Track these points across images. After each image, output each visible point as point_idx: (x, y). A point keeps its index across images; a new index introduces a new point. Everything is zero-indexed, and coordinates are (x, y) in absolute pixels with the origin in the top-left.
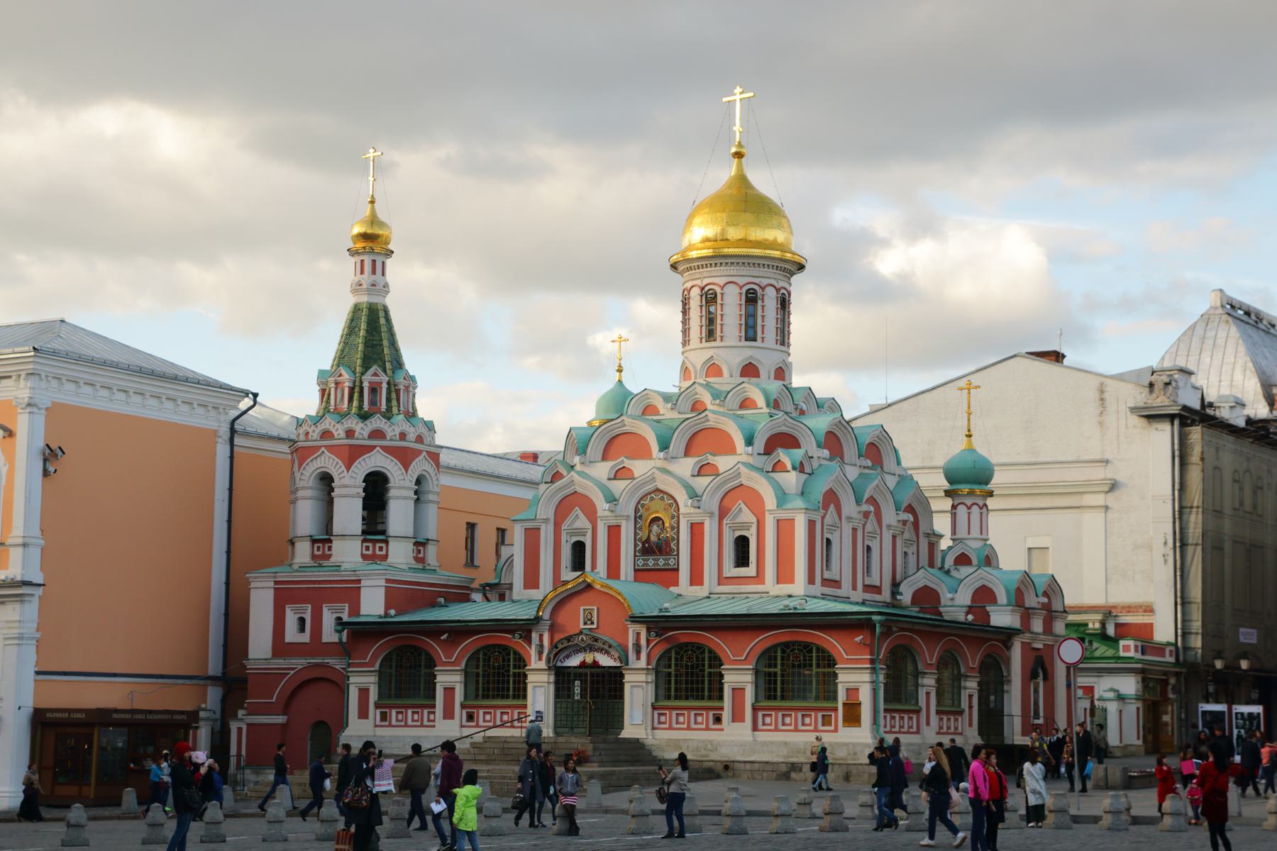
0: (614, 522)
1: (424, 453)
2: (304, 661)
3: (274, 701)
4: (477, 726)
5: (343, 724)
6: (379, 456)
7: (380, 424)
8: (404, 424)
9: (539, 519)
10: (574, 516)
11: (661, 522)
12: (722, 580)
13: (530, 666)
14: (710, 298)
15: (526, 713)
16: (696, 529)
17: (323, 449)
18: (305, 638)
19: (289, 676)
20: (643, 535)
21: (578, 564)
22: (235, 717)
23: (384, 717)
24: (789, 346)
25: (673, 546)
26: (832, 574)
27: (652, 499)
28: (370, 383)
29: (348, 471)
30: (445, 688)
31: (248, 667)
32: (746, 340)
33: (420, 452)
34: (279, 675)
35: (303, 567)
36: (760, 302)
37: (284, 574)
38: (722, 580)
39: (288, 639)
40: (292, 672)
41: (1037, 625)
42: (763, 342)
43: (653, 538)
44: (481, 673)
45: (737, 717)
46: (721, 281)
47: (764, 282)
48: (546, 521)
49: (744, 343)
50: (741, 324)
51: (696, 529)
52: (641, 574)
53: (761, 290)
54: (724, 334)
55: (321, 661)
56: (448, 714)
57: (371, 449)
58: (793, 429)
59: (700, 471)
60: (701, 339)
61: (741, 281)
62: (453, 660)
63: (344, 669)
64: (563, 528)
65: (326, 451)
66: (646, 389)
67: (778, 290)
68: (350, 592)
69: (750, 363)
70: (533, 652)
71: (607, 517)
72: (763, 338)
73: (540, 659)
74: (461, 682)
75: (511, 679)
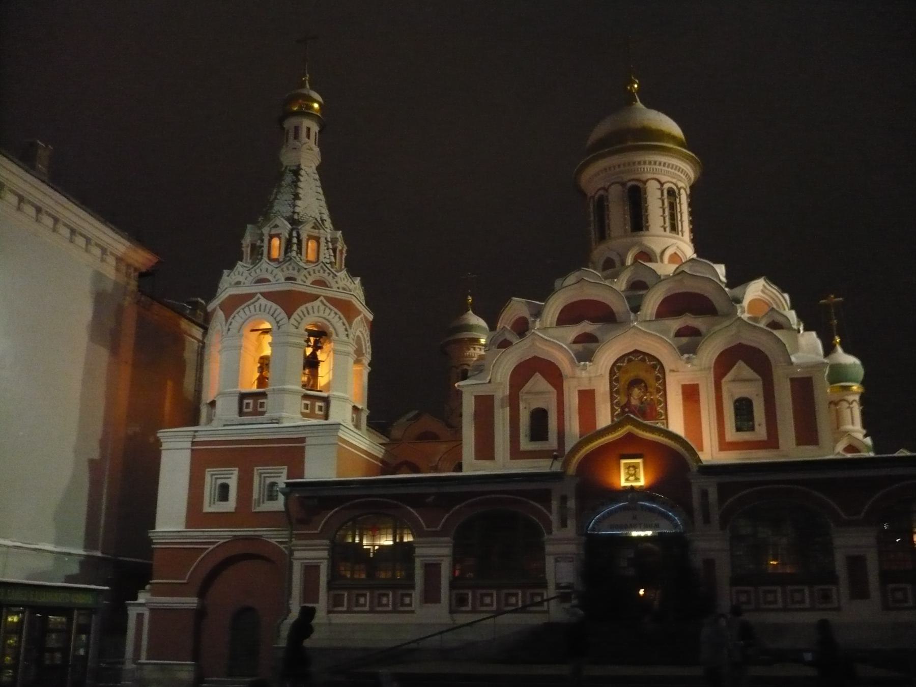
1: (362, 315)
2: (230, 533)
3: (185, 581)
4: (474, 611)
6: (322, 308)
7: (324, 273)
8: (345, 278)
11: (643, 385)
13: (550, 532)
15: (542, 595)
17: (259, 295)
18: (230, 505)
19: (205, 553)
20: (621, 399)
25: (659, 409)
27: (630, 361)
28: (308, 235)
29: (289, 318)
31: (154, 541)
32: (670, 232)
36: (678, 200)
37: (205, 431)
39: (207, 509)
40: (212, 547)
42: (682, 235)
43: (634, 402)
45: (859, 591)
47: (680, 184)
49: (668, 233)
51: (691, 394)
55: (252, 533)
56: (432, 595)
57: (315, 297)
61: (663, 179)
62: (439, 529)
63: (281, 543)
65: (262, 298)
69: (675, 253)
70: (554, 518)
73: (564, 524)
74: (450, 556)
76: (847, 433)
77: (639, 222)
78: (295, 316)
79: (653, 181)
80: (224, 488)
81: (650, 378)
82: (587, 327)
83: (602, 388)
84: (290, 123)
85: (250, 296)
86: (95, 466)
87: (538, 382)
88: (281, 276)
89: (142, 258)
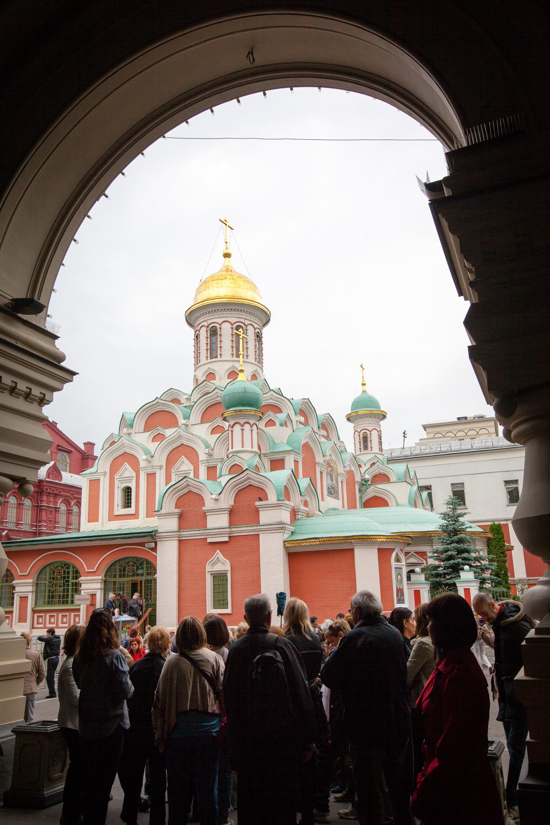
0: (150, 471)
9: (98, 473)
10: (124, 469)
14: (214, 332)
24: (262, 363)
30: (21, 597)
42: (247, 358)
44: (47, 584)
46: (220, 321)
47: (247, 322)
48: (105, 474)
50: (232, 347)
53: (245, 327)
54: (222, 353)
58: (277, 401)
59: (213, 432)
60: (207, 357)
61: (233, 320)
64: (116, 477)
66: (171, 388)
67: (255, 329)
71: (145, 467)
72: (247, 356)
75: (70, 588)
79: (223, 323)
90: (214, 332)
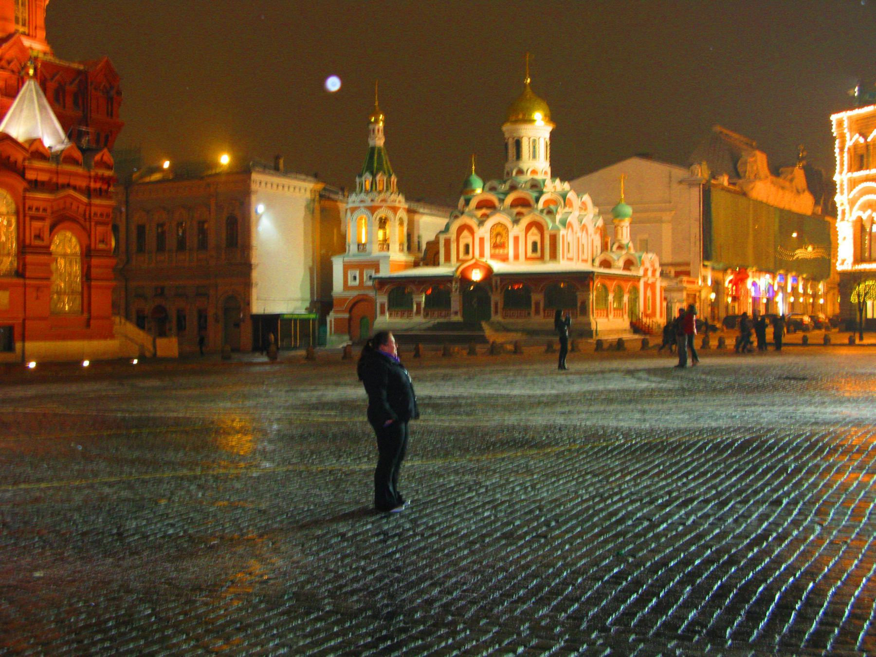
5: (375, 317)
12: (527, 258)
16: (516, 239)
21: (467, 251)
22: (328, 313)
23: (390, 315)
26: (570, 256)
33: (399, 208)
34: (345, 300)
35: (354, 255)
38: (527, 258)
41: (650, 273)
45: (537, 312)
52: (493, 256)
57: (381, 207)
61: (530, 134)
68: (376, 266)
76: (619, 240)
77: (519, 156)
78: (375, 215)
80: (355, 278)
81: (504, 233)
82: (484, 211)
83: (487, 237)
84: (371, 127)
85: (359, 207)
86: (311, 270)
87: (466, 233)
88: (369, 200)
89: (320, 186)
90: (518, 144)
